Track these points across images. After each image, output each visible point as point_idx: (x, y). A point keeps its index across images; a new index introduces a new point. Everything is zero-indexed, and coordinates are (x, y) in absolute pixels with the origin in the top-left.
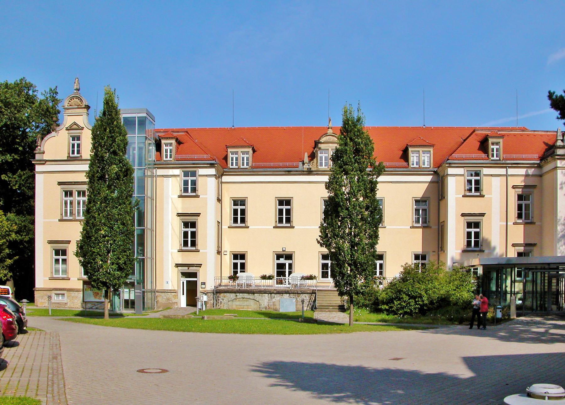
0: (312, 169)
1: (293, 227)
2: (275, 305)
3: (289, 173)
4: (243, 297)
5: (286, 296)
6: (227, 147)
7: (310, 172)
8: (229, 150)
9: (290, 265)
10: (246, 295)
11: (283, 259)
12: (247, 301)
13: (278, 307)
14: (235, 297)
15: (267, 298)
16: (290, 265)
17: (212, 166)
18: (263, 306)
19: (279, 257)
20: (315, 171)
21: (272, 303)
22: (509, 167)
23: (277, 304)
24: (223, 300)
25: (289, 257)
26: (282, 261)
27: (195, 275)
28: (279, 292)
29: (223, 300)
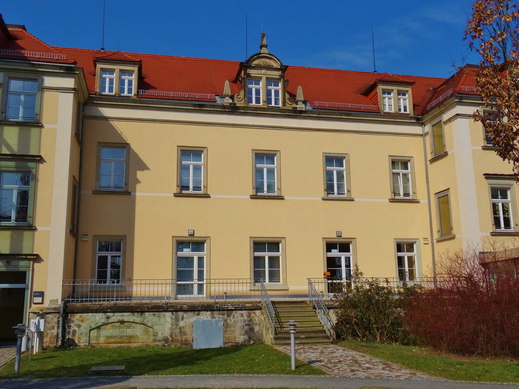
0: (238, 105)
1: (208, 197)
2: (185, 334)
3: (200, 106)
4: (121, 318)
5: (206, 316)
7: (233, 110)
8: (99, 66)
9: (201, 259)
10: (127, 316)
11: (188, 250)
12: (129, 327)
13: (189, 337)
14: (104, 320)
15: (169, 319)
16: (201, 259)
17: (69, 72)
18: (160, 336)
19: (181, 244)
20: (243, 108)
21: (178, 331)
23: (188, 330)
24: (79, 326)
25: (198, 245)
26: (187, 252)
27: (21, 277)
28: (195, 309)
29: (79, 326)
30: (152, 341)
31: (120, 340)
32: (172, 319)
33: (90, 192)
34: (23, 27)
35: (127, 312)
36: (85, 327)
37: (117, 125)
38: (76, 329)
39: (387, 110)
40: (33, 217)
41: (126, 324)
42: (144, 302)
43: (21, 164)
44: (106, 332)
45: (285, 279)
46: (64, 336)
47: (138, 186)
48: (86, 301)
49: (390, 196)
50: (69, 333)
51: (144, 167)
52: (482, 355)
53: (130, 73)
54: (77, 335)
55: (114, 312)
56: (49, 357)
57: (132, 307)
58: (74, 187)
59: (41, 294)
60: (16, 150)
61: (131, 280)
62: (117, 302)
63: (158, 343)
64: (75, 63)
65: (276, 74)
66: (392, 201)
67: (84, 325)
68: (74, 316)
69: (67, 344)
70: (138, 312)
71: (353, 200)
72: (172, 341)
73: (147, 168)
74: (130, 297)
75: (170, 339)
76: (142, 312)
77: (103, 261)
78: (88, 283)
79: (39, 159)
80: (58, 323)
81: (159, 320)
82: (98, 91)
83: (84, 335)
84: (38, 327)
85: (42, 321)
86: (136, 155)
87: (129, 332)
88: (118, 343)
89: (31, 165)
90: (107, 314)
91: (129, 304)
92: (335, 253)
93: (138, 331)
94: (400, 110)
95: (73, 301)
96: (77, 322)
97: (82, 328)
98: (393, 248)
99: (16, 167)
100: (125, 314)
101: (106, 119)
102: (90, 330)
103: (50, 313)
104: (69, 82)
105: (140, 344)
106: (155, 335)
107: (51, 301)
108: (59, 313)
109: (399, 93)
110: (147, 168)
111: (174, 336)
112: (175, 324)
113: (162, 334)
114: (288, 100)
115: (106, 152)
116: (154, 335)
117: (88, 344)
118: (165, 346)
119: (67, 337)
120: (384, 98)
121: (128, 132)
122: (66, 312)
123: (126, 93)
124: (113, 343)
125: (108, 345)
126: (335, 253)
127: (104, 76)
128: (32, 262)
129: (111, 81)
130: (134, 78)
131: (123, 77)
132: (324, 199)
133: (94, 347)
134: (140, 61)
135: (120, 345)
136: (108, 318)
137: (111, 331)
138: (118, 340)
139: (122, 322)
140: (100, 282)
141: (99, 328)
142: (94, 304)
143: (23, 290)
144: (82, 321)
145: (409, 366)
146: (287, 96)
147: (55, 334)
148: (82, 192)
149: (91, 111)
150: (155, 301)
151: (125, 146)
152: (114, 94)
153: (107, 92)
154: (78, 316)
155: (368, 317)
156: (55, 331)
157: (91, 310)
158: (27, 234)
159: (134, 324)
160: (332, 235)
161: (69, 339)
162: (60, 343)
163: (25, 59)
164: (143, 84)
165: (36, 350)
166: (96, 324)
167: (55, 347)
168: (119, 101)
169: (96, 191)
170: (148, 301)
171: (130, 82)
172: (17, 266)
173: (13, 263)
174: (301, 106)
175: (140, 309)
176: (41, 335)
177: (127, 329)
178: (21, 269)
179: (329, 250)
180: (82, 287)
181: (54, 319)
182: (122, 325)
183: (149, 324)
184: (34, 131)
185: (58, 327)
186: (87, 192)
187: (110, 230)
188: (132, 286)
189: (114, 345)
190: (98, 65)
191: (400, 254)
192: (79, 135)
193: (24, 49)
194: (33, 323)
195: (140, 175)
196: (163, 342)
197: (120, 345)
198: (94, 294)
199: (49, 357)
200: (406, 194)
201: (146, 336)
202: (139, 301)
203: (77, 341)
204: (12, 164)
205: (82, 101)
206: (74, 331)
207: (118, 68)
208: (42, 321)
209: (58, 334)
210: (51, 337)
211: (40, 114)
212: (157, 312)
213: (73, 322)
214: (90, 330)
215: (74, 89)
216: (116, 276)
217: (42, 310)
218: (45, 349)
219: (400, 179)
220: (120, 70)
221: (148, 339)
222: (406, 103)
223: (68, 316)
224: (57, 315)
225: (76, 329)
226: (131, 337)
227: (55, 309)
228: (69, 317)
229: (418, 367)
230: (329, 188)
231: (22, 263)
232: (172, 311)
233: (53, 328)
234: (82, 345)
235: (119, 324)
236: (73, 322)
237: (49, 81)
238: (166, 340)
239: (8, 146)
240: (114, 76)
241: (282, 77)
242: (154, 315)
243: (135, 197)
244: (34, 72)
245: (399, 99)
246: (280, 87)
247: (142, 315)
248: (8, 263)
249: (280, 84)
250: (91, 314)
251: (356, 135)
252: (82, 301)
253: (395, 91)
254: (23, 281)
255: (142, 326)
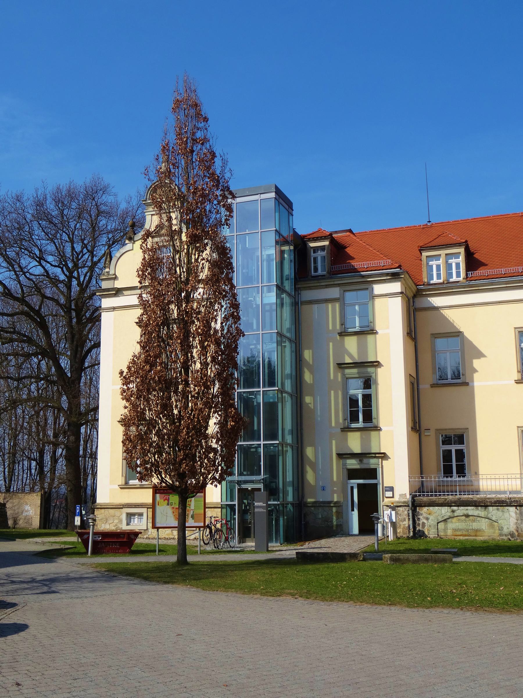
4: (465, 512)
6: (420, 251)
8: (425, 254)
10: (471, 510)
12: (474, 521)
14: (449, 514)
15: (513, 514)
17: (395, 277)
18: (505, 531)
24: (427, 519)
27: (372, 473)
29: (427, 519)
30: (498, 535)
31: (467, 533)
32: (516, 513)
33: (428, 386)
34: (350, 231)
35: (471, 506)
36: (431, 518)
37: (447, 313)
38: (425, 521)
40: (377, 418)
41: (471, 518)
42: (489, 496)
43: (362, 370)
44: (453, 525)
46: (414, 528)
47: (476, 375)
48: (432, 495)
50: (419, 525)
51: (480, 355)
53: (456, 255)
54: (426, 527)
55: (458, 506)
56: (401, 543)
57: (476, 501)
58: (412, 384)
59: (391, 489)
60: (357, 359)
61: (477, 473)
62: (462, 496)
63: (504, 537)
64: (399, 267)
67: (431, 517)
68: (422, 510)
69: (418, 534)
70: (481, 506)
72: (518, 536)
73: (484, 356)
74: (478, 492)
75: (517, 534)
76: (486, 506)
77: (447, 456)
78: (434, 478)
79: (376, 364)
80: (409, 516)
81: (503, 515)
82: (426, 280)
83: (432, 527)
84: (390, 518)
85: (393, 513)
86: (471, 343)
87: (475, 526)
88: (465, 536)
89: (371, 370)
90: (452, 508)
91: (472, 499)
93: (483, 525)
95: (420, 495)
96: (425, 515)
97: (430, 521)
99: (358, 373)
100: (469, 508)
101: (436, 309)
102: (438, 523)
103: (400, 506)
104: (396, 287)
105: (486, 538)
106: (501, 529)
107: (400, 495)
108: (408, 506)
110: (484, 356)
111: (520, 531)
112: (520, 519)
113: (508, 528)
115: (440, 343)
116: (499, 530)
117: (437, 536)
118: (510, 540)
119: (418, 529)
121: (458, 319)
122: (415, 505)
123: (454, 278)
124: (460, 535)
125: (456, 537)
127: (431, 263)
128: (380, 460)
129: (438, 267)
130: (461, 260)
131: (450, 261)
133: (442, 538)
134: (466, 241)
135: (467, 538)
136: (453, 511)
137: (457, 524)
138: (464, 533)
139: (467, 516)
140: (447, 477)
141: (445, 521)
142: (439, 499)
143: (375, 486)
144: (429, 514)
147: (407, 525)
148: (421, 386)
149: (421, 302)
150: (499, 496)
151: (458, 334)
152: (441, 281)
153: (435, 280)
154: (425, 509)
156: (406, 523)
157: (436, 504)
158: (373, 434)
159: (479, 519)
161: (419, 530)
162: (411, 534)
163: (355, 270)
164: (472, 263)
165: (391, 538)
166: (443, 517)
167: (408, 537)
168: (448, 288)
169: (433, 384)
170: (494, 496)
171: (458, 265)
172: (368, 464)
173: (365, 461)
175: (484, 504)
176: (394, 525)
177: (472, 522)
178: (372, 467)
180: (427, 481)
181: (404, 512)
182: (467, 519)
183: (494, 519)
184: (370, 338)
185: (409, 519)
186: (425, 386)
187: (452, 424)
188: (478, 481)
189: (461, 538)
190: (423, 254)
192: (412, 333)
193: (353, 258)
194: (386, 515)
195: (477, 363)
196: (509, 537)
197: (467, 538)
198: (440, 489)
199: (401, 543)
201: (491, 530)
202: (485, 496)
203: (426, 533)
204: (355, 371)
205: (410, 295)
206: (424, 524)
207: (443, 252)
208: (393, 513)
209: (409, 526)
210: (404, 528)
211: (373, 322)
212: (501, 506)
213: (422, 514)
214: (438, 523)
215: (402, 293)
216: (461, 471)
217: (392, 503)
218: (399, 538)
220: (446, 254)
221: (494, 533)
223: (416, 509)
224: (407, 508)
225: (425, 521)
226: (477, 531)
227: (404, 502)
228: (418, 510)
231: (373, 461)
232: (516, 506)
233: (405, 520)
234: (431, 536)
235: (464, 518)
236: (422, 514)
237: (378, 289)
238: (512, 535)
239: (351, 356)
240: (441, 262)
242: (498, 509)
243: (473, 387)
244: (364, 283)
247: (485, 509)
248: (361, 461)
250: (437, 508)
252: (428, 495)
254: (375, 477)
255: (487, 520)
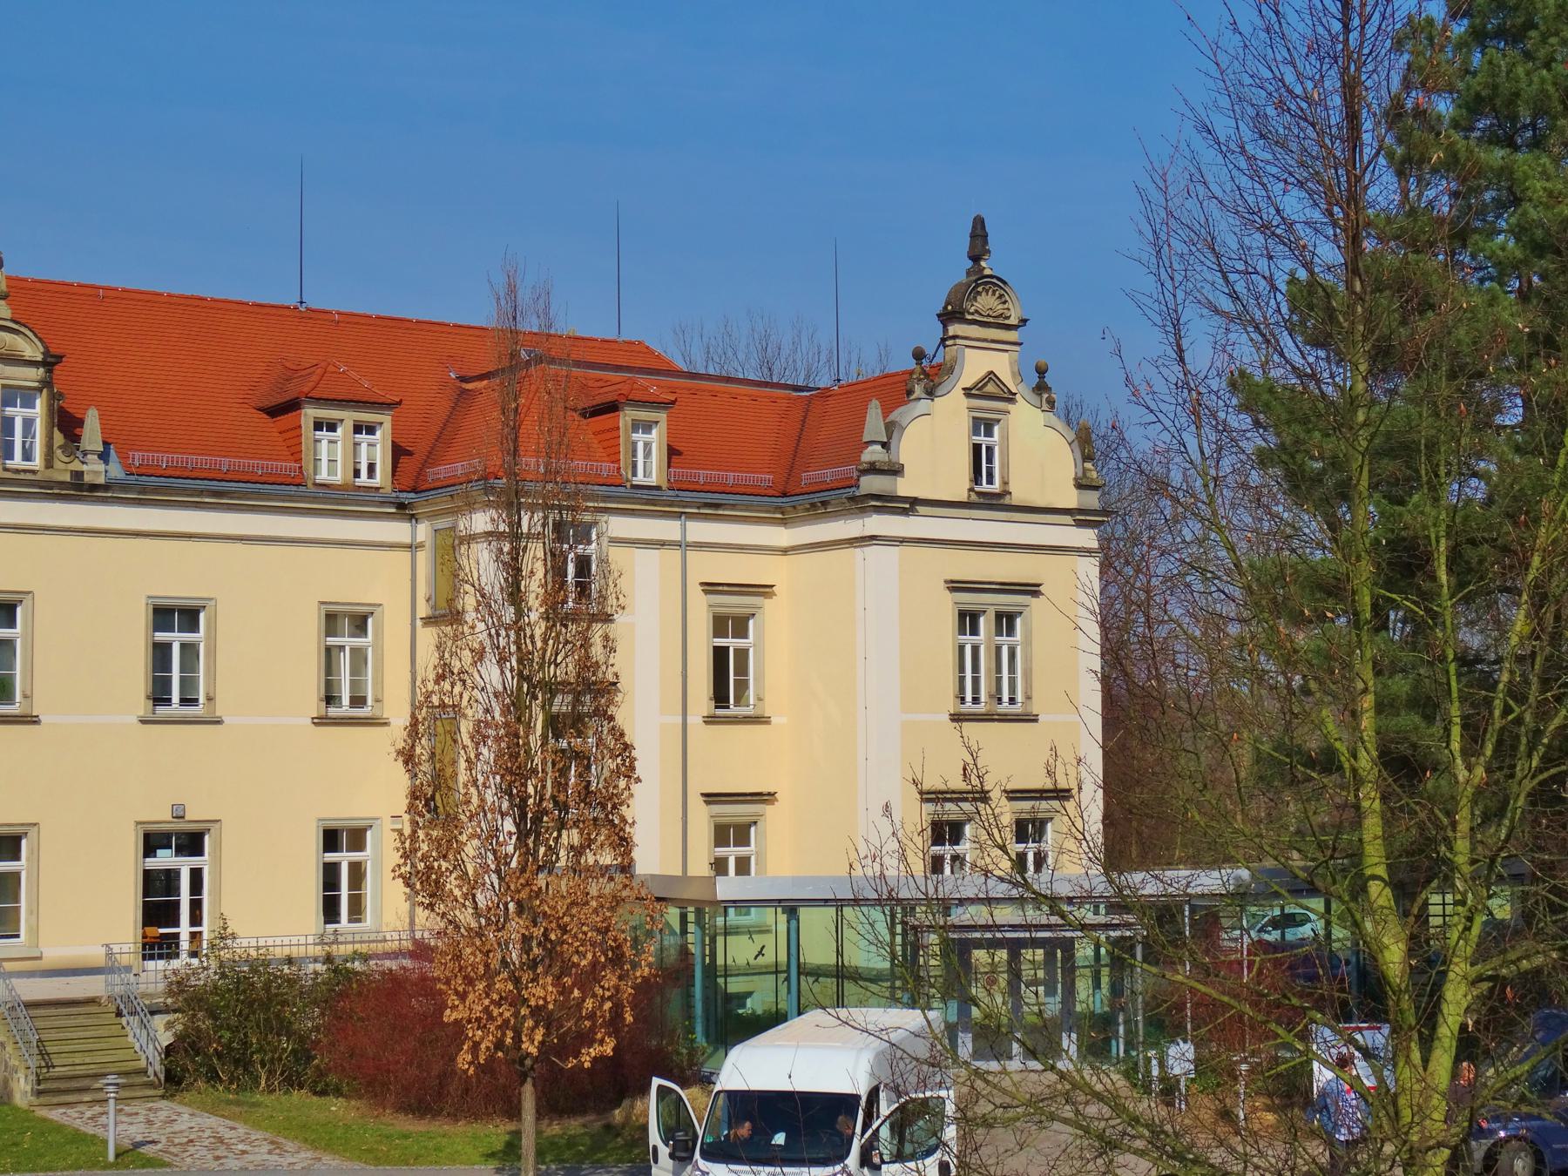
22: (691, 516)
39: (323, 476)
45: (35, 931)
49: (314, 706)
52: (454, 1117)
65: (32, 376)
66: (321, 721)
71: (219, 722)
92: (165, 859)
94: (357, 473)
98: (315, 840)
109: (358, 429)
114: (59, 452)
120: (317, 441)
126: (165, 859)
132: (143, 722)
145: (314, 1145)
146: (59, 438)
155: (242, 1035)
160: (160, 815)
174: (94, 470)
179: (149, 851)
191: (331, 857)
200: (358, 701)
219: (345, 662)
222: (377, 449)
229: (329, 1147)
230: (160, 696)
241: (46, 383)
245: (356, 445)
246: (40, 404)
249: (38, 402)
251: (239, 546)
253: (349, 425)
